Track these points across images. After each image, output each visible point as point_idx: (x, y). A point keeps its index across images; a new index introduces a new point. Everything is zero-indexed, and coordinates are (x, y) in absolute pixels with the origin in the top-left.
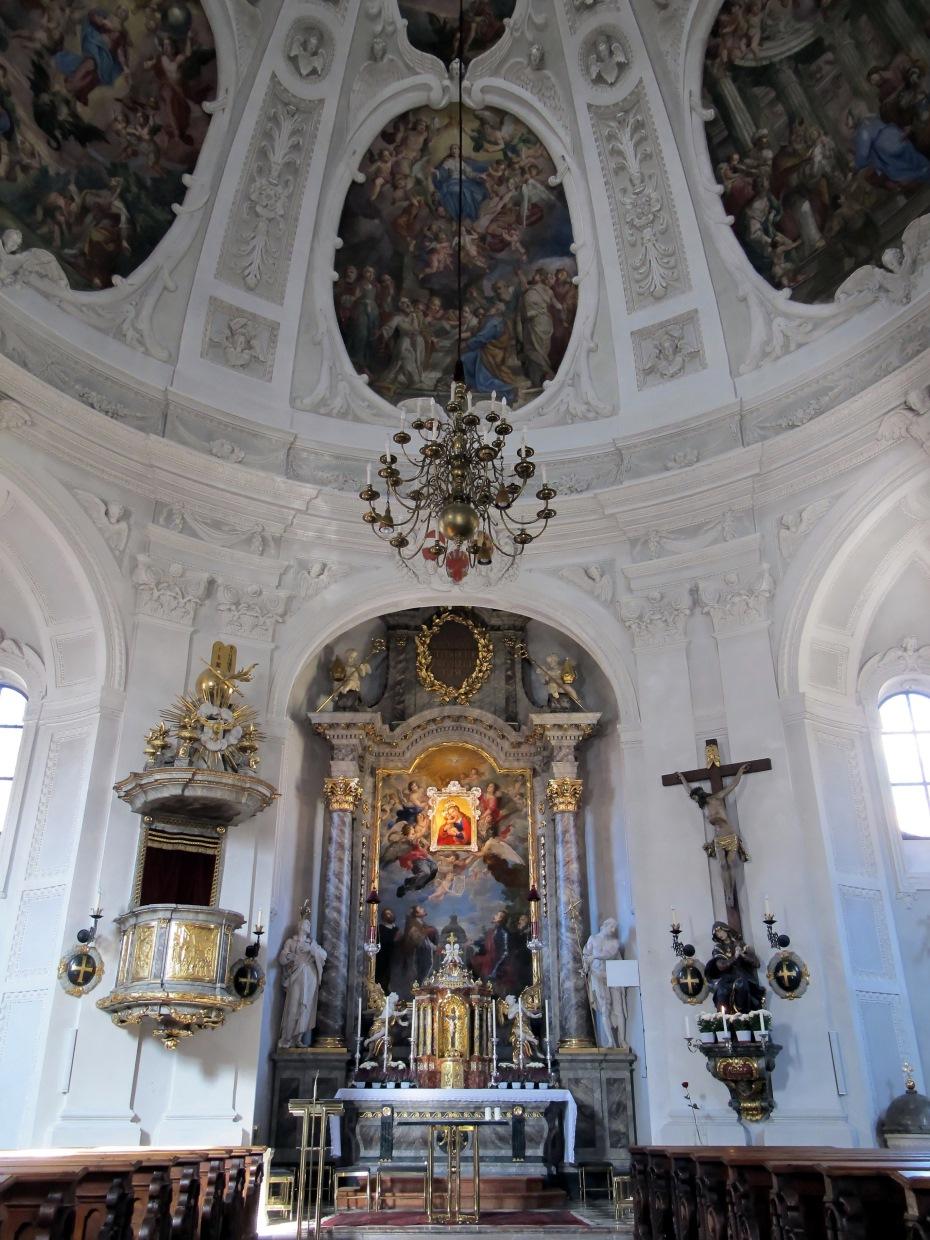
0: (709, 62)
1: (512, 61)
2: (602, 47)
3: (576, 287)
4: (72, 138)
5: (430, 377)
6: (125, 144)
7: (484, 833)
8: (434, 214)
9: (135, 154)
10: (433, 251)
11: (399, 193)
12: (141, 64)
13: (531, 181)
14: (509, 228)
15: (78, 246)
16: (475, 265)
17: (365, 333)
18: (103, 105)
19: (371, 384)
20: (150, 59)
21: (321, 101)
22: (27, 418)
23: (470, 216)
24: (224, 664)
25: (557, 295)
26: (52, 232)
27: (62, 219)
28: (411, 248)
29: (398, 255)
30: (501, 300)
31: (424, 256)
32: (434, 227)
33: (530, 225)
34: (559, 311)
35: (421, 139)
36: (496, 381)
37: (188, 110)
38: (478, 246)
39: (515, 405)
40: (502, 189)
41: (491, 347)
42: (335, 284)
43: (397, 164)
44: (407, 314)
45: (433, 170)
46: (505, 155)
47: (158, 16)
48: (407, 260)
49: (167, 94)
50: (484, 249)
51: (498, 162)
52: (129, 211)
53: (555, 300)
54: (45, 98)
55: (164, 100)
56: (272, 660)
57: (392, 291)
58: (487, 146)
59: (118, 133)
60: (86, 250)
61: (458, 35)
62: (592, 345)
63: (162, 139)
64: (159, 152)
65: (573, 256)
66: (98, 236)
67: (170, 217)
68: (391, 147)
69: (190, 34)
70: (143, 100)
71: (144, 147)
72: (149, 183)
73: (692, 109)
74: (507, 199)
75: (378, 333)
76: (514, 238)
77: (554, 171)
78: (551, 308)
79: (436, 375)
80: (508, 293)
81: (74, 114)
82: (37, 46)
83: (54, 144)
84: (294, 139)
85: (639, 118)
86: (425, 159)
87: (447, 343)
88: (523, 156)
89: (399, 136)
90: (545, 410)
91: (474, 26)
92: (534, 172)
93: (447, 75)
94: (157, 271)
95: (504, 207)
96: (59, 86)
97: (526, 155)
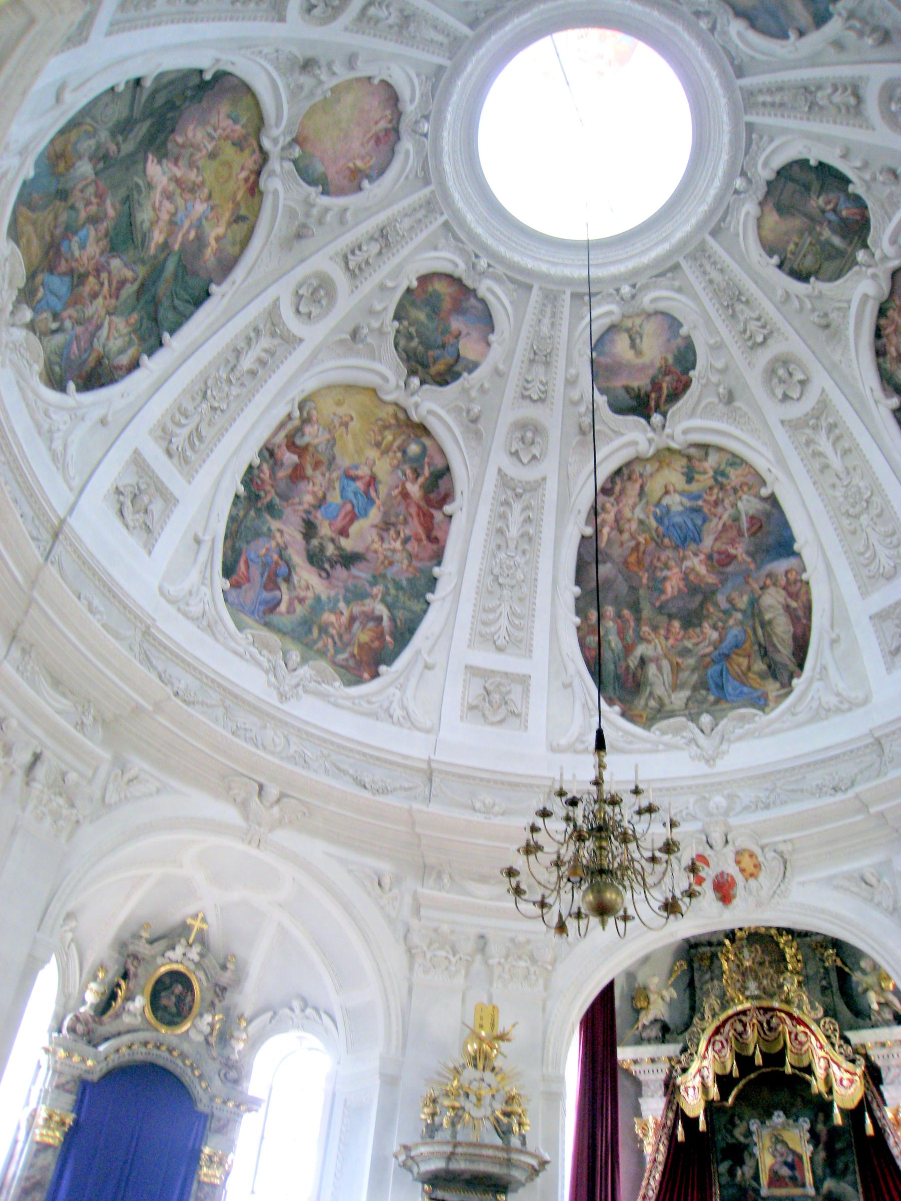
0: (881, 360)
1: (703, 404)
2: (781, 372)
3: (807, 583)
4: (338, 567)
5: (679, 698)
6: (381, 558)
7: (820, 1172)
8: (660, 545)
9: (391, 564)
10: (665, 579)
11: (626, 536)
12: (389, 495)
13: (745, 497)
14: (732, 542)
15: (349, 649)
16: (707, 584)
17: (612, 667)
18: (363, 534)
19: (623, 715)
20: (397, 487)
21: (544, 479)
22: (305, 810)
23: (695, 541)
24: (487, 1026)
25: (790, 595)
26: (326, 645)
27: (333, 632)
28: (645, 581)
29: (633, 589)
30: (736, 610)
31: (657, 586)
32: (663, 558)
33: (753, 534)
34: (795, 609)
35: (637, 486)
36: (746, 690)
37: (432, 516)
38: (706, 565)
39: (767, 709)
40: (720, 510)
41: (734, 656)
42: (578, 629)
43: (619, 513)
44: (649, 642)
45: (652, 508)
46: (716, 480)
47: (399, 455)
48: (642, 592)
49: (413, 510)
50: (713, 567)
51: (711, 488)
52: (390, 607)
53: (789, 600)
54: (315, 542)
55: (411, 515)
56: (544, 1009)
57: (632, 624)
58: (697, 476)
59: (376, 552)
60: (356, 652)
61: (653, 395)
62: (833, 636)
63: (412, 546)
64: (410, 556)
65: (797, 555)
66: (364, 637)
67: (425, 606)
68: (612, 499)
69: (426, 460)
70: (393, 519)
71: (398, 556)
72: (404, 583)
73: (876, 402)
74: (725, 517)
75: (623, 664)
76: (739, 551)
77: (764, 483)
78: (787, 608)
79: (686, 693)
80: (743, 602)
81: (339, 548)
82: (306, 506)
83: (324, 574)
84: (525, 515)
85: (831, 420)
86: (644, 501)
87: (691, 661)
88: (733, 477)
89: (617, 489)
90: (798, 709)
91: (665, 385)
92: (745, 489)
93: (649, 429)
94: (418, 652)
95: (724, 525)
96: (325, 530)
97: (735, 476)
